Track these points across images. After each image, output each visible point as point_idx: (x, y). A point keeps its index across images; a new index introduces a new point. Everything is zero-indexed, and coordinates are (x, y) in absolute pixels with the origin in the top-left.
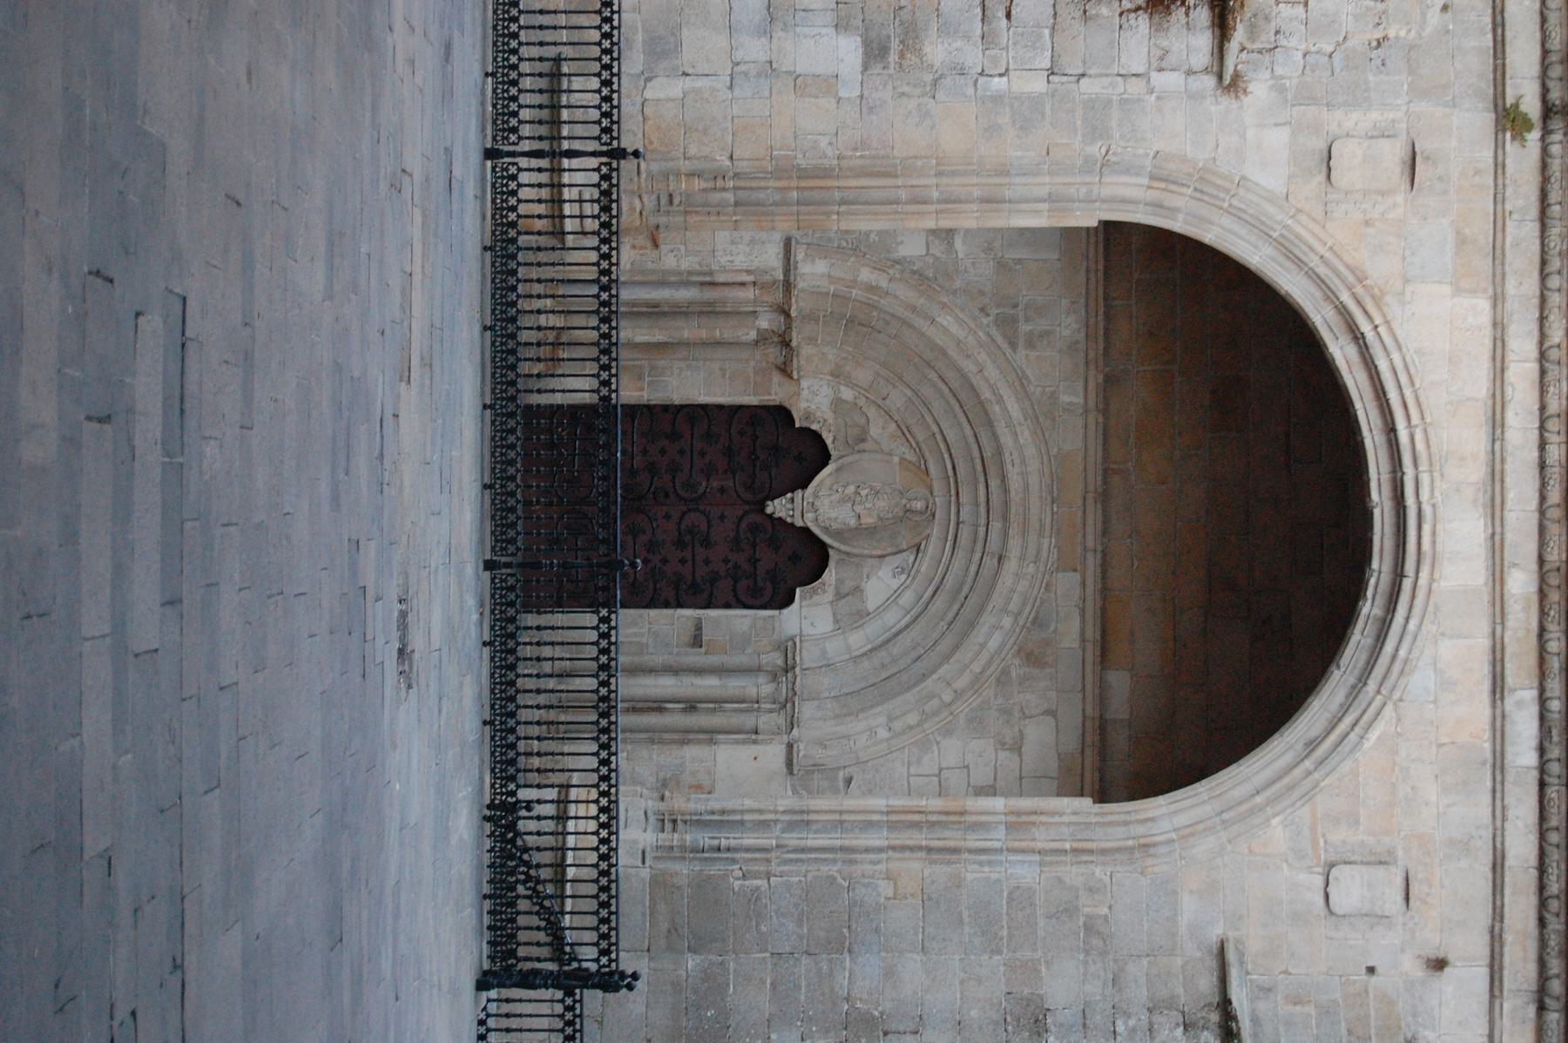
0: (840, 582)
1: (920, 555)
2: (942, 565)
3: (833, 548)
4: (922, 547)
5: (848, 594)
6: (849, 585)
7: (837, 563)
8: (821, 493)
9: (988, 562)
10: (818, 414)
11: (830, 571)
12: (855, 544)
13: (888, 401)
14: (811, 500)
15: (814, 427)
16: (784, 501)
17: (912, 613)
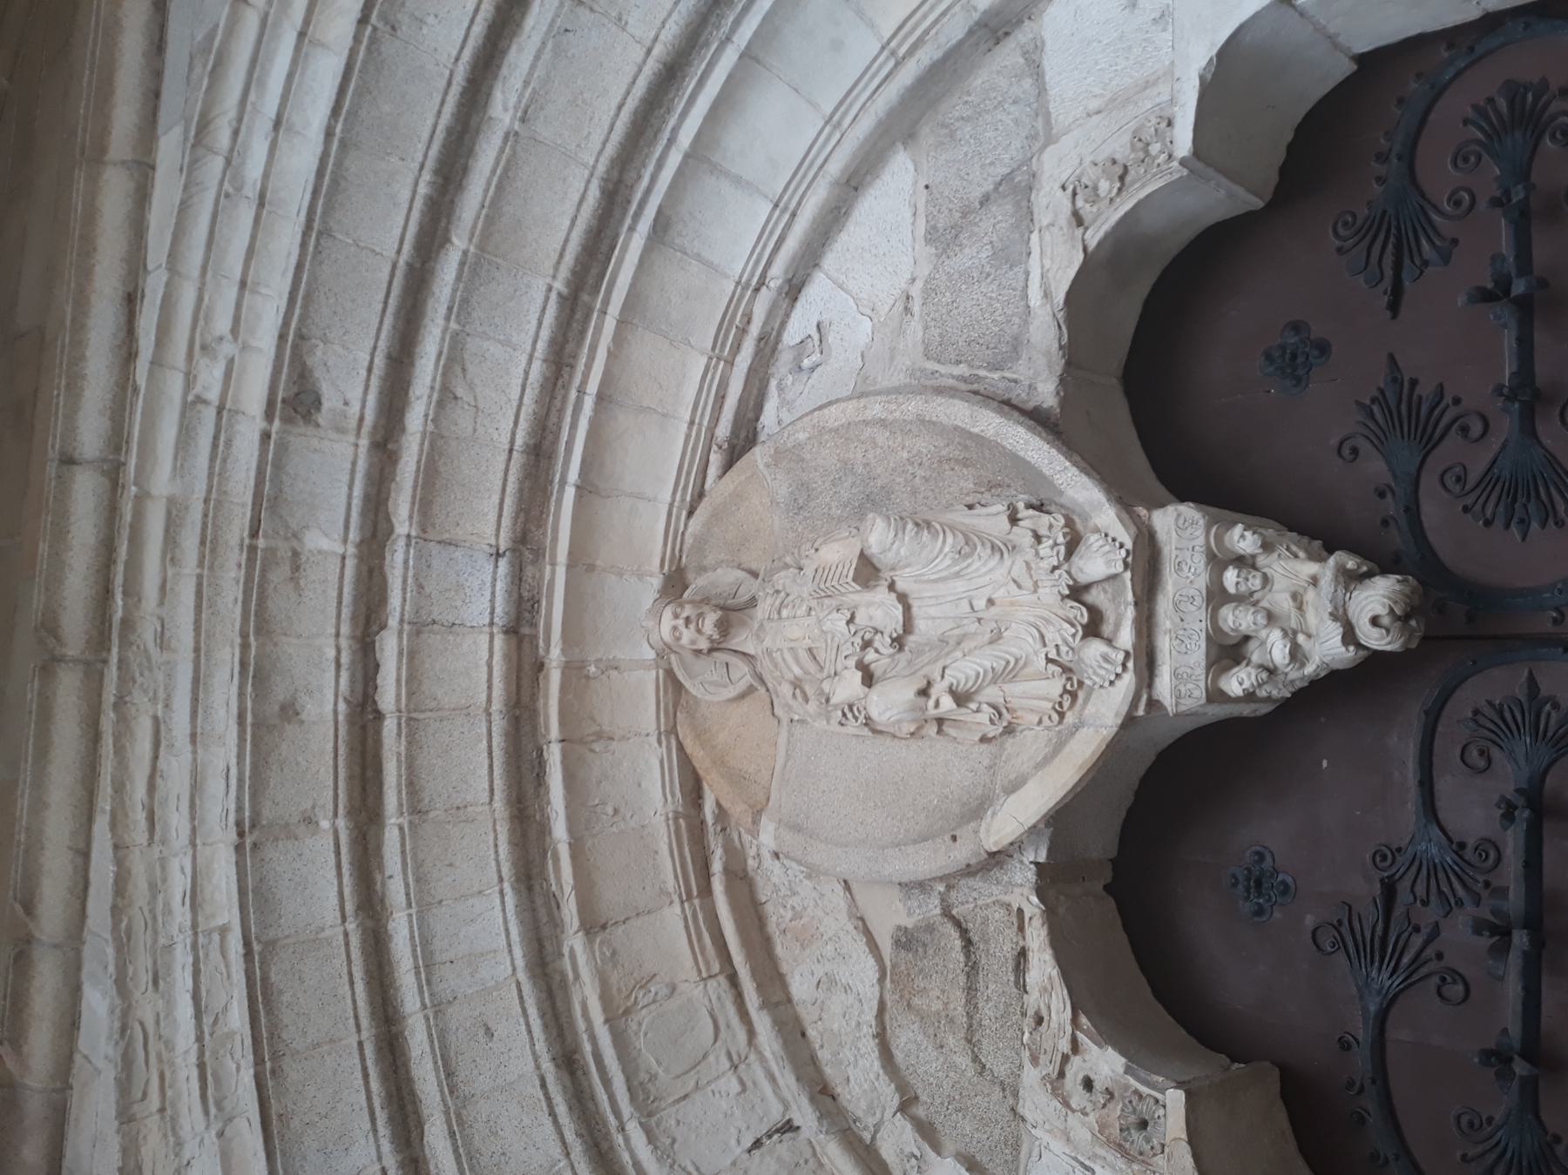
0: (1010, 255)
1: (723, 430)
2: (593, 387)
3: (1037, 418)
4: (716, 459)
5: (985, 200)
6: (972, 255)
7: (1017, 345)
8: (1055, 687)
9: (355, 395)
10: (1082, 1131)
11: (1047, 295)
12: (923, 444)
13: (776, 1115)
14: (1096, 648)
15: (1106, 1063)
16: (1279, 652)
17: (674, 160)
